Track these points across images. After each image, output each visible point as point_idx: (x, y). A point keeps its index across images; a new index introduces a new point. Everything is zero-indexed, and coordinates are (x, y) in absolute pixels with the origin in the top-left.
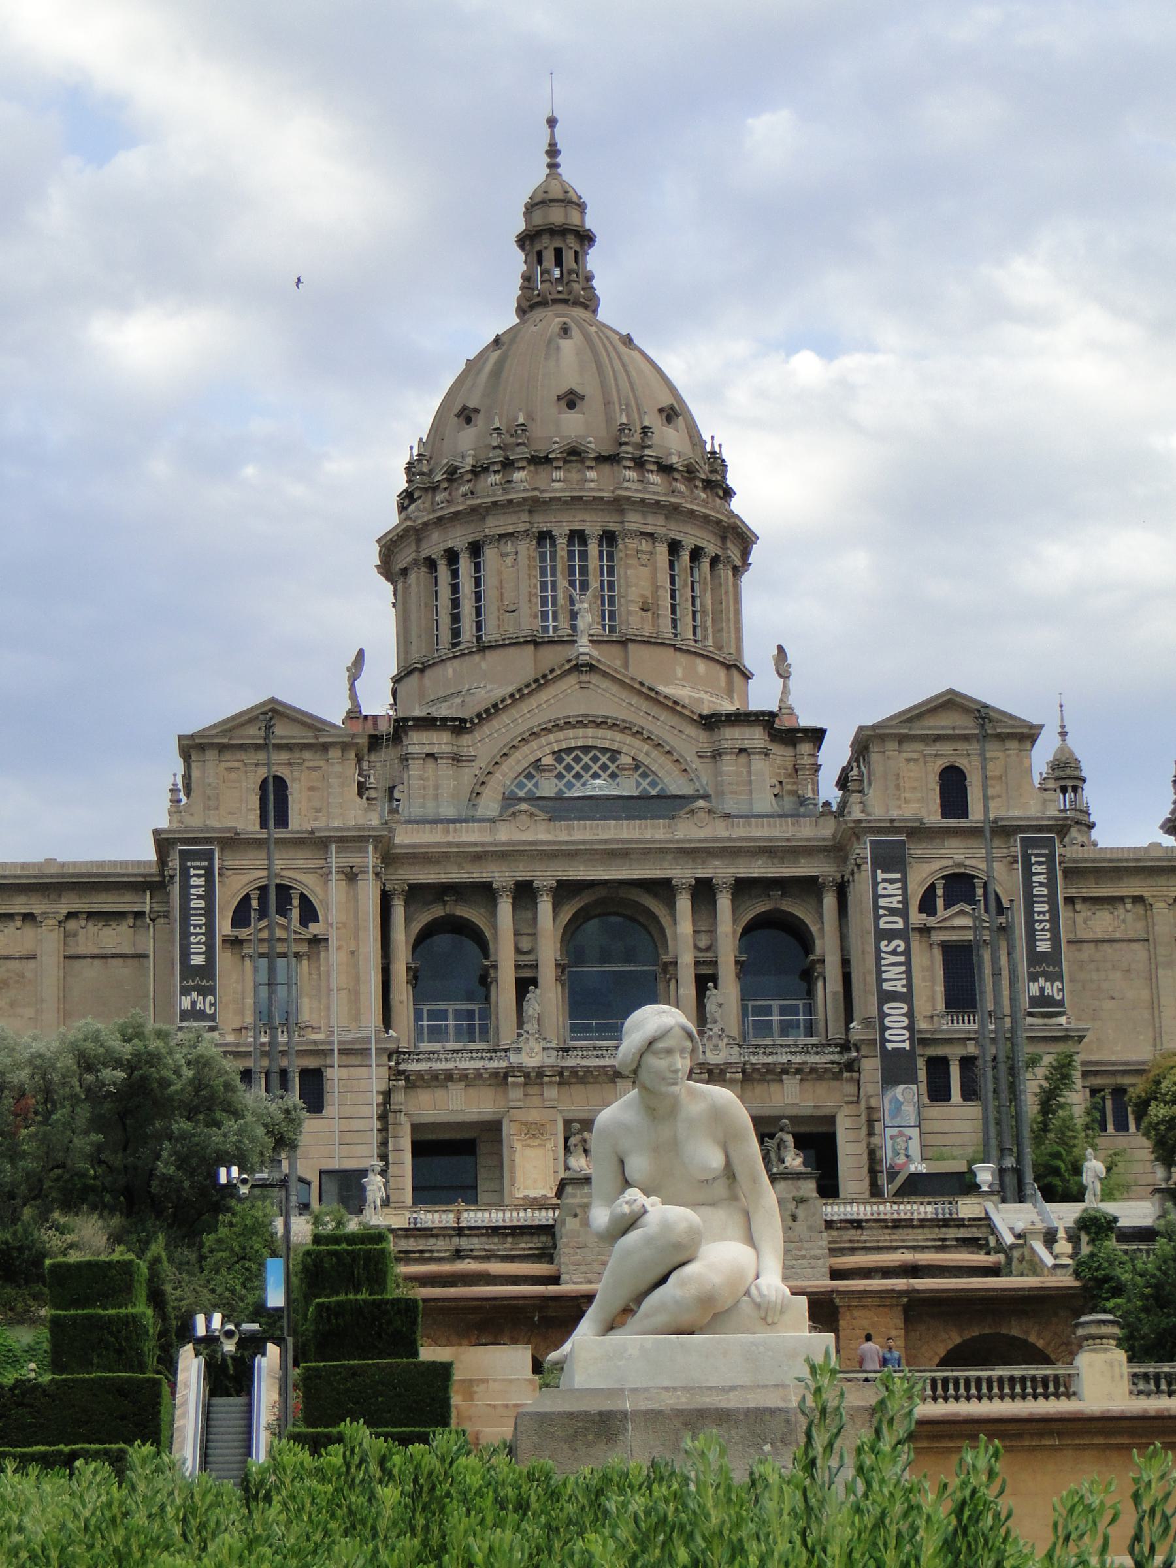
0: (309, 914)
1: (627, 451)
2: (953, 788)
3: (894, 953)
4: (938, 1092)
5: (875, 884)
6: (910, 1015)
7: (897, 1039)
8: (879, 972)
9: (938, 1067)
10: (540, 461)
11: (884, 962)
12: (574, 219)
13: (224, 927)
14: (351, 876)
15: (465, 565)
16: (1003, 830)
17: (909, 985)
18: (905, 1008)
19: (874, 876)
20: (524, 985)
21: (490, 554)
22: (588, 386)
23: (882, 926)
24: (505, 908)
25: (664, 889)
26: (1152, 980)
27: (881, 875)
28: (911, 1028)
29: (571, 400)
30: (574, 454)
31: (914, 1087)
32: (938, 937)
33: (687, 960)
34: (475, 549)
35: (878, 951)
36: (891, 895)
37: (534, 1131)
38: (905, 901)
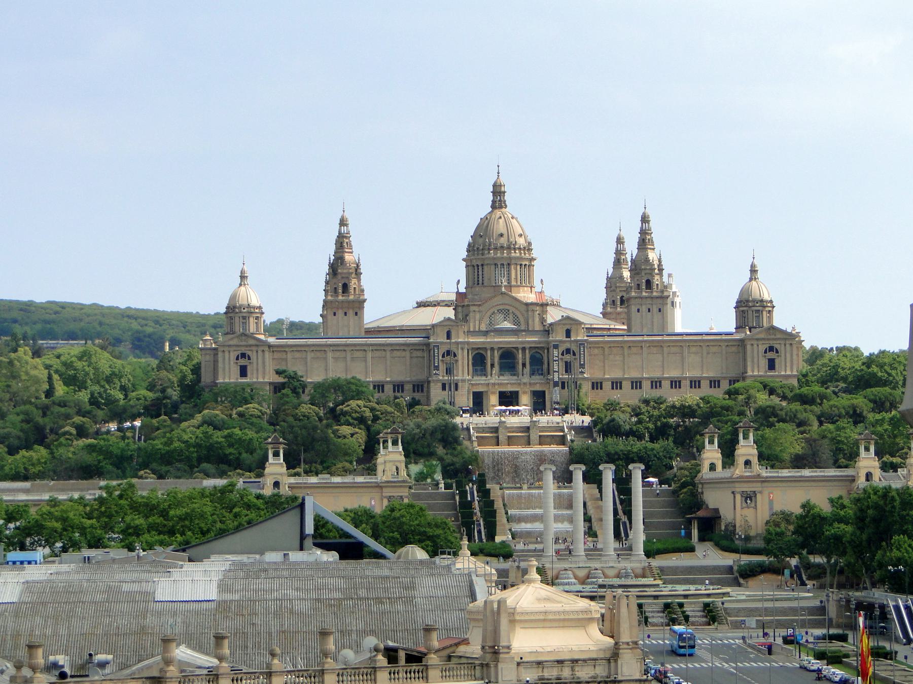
0: (455, 355)
1: (511, 247)
2: (568, 333)
4: (563, 387)
7: (556, 379)
9: (563, 383)
10: (496, 249)
12: (503, 189)
13: (440, 358)
14: (462, 349)
15: (480, 268)
16: (576, 341)
20: (492, 365)
21: (485, 267)
22: (504, 232)
24: (489, 352)
25: (517, 349)
26: (604, 362)
29: (502, 235)
30: (502, 247)
33: (520, 362)
34: (482, 265)
36: (556, 353)
37: (493, 393)
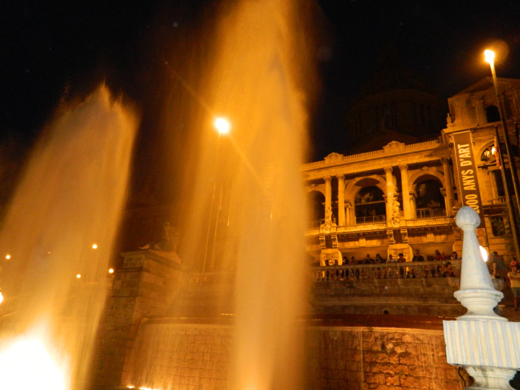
3: (469, 175)
5: (458, 150)
6: (479, 199)
8: (462, 183)
11: (463, 179)
17: (477, 186)
18: (476, 196)
19: (457, 147)
23: (462, 165)
25: (381, 172)
27: (459, 146)
28: (480, 204)
31: (484, 229)
32: (491, 169)
35: (461, 175)
38: (472, 154)
